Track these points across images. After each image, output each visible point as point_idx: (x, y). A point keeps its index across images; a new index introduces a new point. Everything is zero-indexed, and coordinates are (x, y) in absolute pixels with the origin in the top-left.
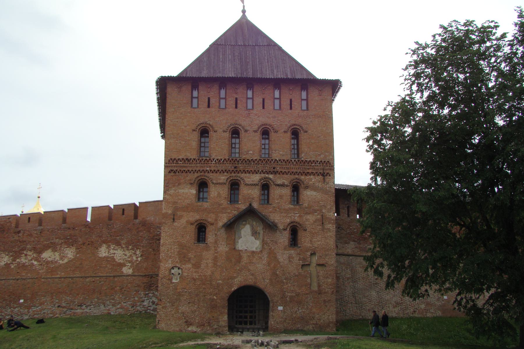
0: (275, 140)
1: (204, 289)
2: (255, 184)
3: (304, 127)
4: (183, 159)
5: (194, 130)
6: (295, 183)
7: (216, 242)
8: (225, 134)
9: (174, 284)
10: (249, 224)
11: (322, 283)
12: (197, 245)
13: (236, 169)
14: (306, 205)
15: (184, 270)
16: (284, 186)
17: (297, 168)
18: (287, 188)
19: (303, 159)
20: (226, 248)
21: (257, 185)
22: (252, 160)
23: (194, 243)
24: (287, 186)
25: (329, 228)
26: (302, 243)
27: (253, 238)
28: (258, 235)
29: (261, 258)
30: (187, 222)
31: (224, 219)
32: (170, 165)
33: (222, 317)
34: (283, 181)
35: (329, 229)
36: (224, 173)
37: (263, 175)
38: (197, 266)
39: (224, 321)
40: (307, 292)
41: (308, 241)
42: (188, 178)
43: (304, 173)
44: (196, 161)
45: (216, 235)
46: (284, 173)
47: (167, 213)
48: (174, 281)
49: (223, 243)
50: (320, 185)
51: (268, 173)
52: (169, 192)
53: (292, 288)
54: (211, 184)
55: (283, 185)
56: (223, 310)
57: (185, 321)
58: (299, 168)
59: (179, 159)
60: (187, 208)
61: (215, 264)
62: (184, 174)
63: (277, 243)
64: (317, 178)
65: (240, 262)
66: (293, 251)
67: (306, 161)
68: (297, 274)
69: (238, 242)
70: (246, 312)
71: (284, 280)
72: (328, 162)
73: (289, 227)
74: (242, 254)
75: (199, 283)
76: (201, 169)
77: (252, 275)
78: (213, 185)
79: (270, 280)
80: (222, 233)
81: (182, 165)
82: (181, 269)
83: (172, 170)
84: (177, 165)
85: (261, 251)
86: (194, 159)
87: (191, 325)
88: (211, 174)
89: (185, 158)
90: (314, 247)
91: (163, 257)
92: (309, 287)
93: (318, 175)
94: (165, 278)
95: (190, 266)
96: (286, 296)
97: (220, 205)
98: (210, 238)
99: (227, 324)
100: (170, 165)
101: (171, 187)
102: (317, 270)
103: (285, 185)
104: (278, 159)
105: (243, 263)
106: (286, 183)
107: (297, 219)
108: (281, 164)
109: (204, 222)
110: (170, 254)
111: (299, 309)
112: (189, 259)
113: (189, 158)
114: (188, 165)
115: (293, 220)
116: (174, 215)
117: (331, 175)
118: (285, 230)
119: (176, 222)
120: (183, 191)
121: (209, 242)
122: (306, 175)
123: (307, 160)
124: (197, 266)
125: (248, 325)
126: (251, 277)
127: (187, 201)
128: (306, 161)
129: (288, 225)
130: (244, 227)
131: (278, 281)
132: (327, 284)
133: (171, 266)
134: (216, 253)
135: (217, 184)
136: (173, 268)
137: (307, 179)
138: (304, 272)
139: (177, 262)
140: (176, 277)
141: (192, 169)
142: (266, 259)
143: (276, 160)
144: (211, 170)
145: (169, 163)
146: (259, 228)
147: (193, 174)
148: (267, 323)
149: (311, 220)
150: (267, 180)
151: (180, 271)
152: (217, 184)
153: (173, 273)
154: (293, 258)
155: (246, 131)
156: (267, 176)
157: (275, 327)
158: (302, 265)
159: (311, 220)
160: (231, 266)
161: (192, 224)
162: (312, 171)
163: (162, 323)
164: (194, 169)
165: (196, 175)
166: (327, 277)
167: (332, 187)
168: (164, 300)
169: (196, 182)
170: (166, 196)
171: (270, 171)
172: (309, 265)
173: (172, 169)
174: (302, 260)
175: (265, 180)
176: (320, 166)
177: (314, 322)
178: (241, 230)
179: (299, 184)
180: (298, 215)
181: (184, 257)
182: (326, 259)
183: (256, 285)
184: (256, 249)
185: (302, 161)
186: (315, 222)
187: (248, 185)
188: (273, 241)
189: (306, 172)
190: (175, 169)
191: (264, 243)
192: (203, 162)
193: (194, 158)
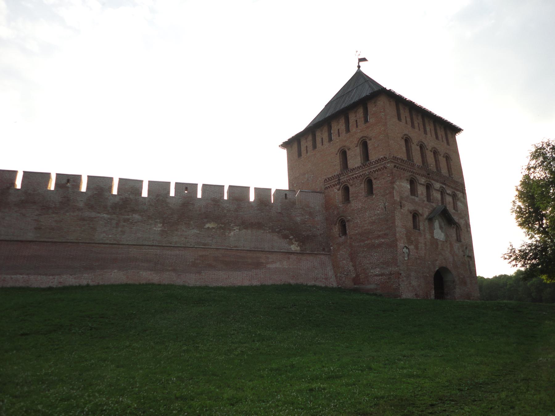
31: (425, 212)
38: (417, 248)
48: (406, 259)
49: (428, 232)
77: (445, 259)
80: (426, 223)
81: (401, 163)
86: (406, 161)
114: (403, 164)
124: (417, 248)
133: (402, 245)
134: (425, 239)
161: (411, 213)
165: (410, 174)
184: (443, 239)
191: (447, 236)
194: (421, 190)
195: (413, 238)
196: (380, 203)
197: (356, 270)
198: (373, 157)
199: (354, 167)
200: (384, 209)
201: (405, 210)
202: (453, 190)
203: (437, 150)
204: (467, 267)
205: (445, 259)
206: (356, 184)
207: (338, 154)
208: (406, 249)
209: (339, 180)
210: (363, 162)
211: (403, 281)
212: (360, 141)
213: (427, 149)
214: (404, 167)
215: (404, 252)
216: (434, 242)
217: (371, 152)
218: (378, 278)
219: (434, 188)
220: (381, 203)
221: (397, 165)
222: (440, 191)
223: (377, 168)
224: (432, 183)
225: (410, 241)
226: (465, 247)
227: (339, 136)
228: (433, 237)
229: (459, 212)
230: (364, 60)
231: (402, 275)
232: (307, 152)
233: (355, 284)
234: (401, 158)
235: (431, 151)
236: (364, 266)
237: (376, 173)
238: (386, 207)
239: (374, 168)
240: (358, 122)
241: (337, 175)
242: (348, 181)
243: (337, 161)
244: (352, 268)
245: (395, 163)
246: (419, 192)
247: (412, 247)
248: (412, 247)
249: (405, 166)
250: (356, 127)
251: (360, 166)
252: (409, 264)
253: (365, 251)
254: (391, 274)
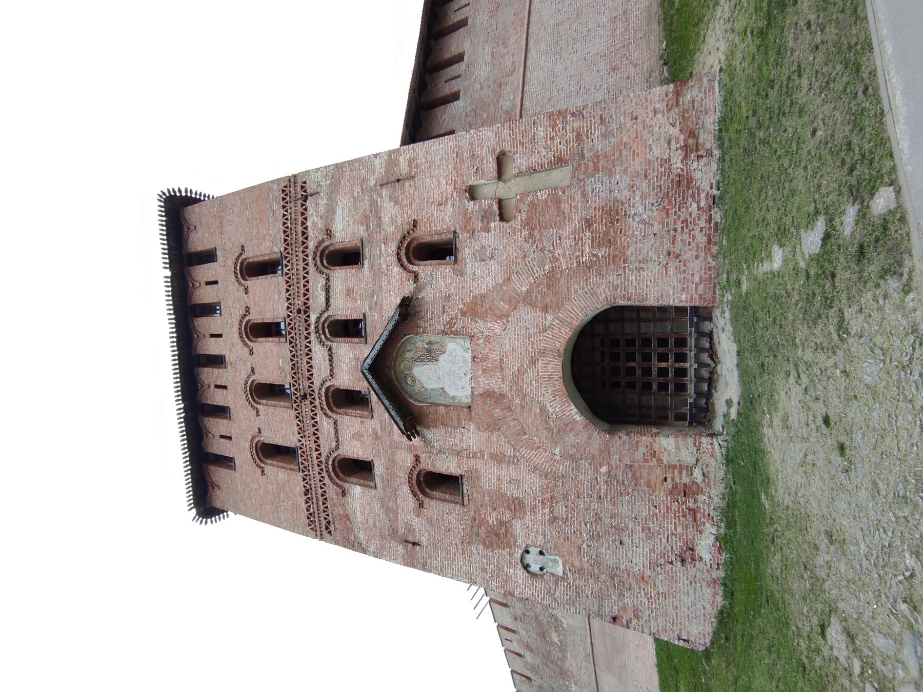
0: (260, 312)
1: (579, 497)
2: (330, 355)
3: (237, 252)
4: (307, 502)
5: (263, 472)
6: (325, 262)
7: (458, 454)
8: (261, 412)
9: (570, 575)
10: (410, 369)
11: (550, 155)
12: (466, 499)
13: (308, 396)
14: (362, 228)
15: (529, 542)
16: (329, 286)
17: (297, 260)
18: (331, 278)
19: (282, 249)
20: (469, 431)
21: (330, 349)
22: (292, 360)
23: (464, 505)
24: (328, 279)
25: (407, 163)
26: (445, 227)
27: (441, 358)
28: (435, 347)
29: (488, 339)
30: (418, 516)
32: (318, 528)
33: (666, 454)
34: (319, 289)
35: (410, 162)
36: (316, 422)
37: (313, 337)
39: (678, 448)
40: (578, 196)
41: (440, 211)
42: (335, 497)
43: (303, 243)
44: (306, 475)
45: (440, 452)
46: (306, 288)
47: (403, 556)
48: (559, 571)
49: (458, 436)
50: (323, 201)
51: (309, 325)
52: (364, 542)
53: (568, 243)
54: (340, 452)
55: (327, 290)
56: (642, 449)
57: (679, 564)
58: (297, 256)
59: (308, 510)
60: (391, 512)
61: (514, 461)
62: (328, 504)
63: (449, 296)
64: (311, 212)
65: (502, 396)
66: (467, 251)
67: (284, 242)
68: (525, 233)
69: (453, 397)
70: (647, 372)
71: (547, 268)
72: (283, 191)
73: (410, 267)
74: (481, 391)
75: (564, 509)
76: (317, 469)
77: (533, 362)
78: (341, 447)
79: (545, 309)
80: (434, 435)
81: (315, 503)
82: (526, 547)
83: (327, 528)
84: (316, 516)
85: (471, 337)
86: (304, 479)
87: (692, 550)
88: (322, 449)
89: (305, 498)
90: (455, 194)
91: (499, 585)
92: (564, 192)
93: (306, 209)
94: (552, 592)
95: (518, 527)
96: (594, 259)
97: (376, 436)
98: (448, 466)
99: (690, 440)
100: (318, 528)
101: (354, 535)
102: (517, 176)
103: (326, 284)
104: (286, 304)
105: (505, 388)
106: (322, 282)
107: (393, 247)
108: (292, 296)
109: (415, 476)
110: (492, 566)
111: (635, 214)
112: (501, 523)
113: (304, 490)
115: (395, 259)
116: (406, 541)
117: (304, 180)
118: (416, 277)
119: (419, 540)
120: (358, 514)
121: (458, 470)
122: (306, 238)
123: (283, 240)
124: (517, 506)
125: (687, 365)
126: (540, 366)
127: (377, 506)
128: (285, 240)
129: (405, 268)
130: (419, 381)
131: (548, 286)
132: (552, 138)
133: (521, 572)
134: (483, 456)
135: (337, 437)
136: (526, 567)
137: (314, 234)
138: (520, 212)
139: (511, 555)
140: (550, 564)
141: (319, 488)
142: (489, 325)
143: (288, 308)
144: (317, 450)
145: (316, 531)
146: (419, 345)
147: (327, 486)
148: (680, 310)
149: (394, 212)
150: (320, 327)
151: (534, 551)
152: (338, 440)
153: (538, 569)
154: (483, 247)
155: (253, 371)
156: (312, 327)
157: (701, 287)
158: (502, 218)
159: (394, 212)
160: (515, 419)
161: (421, 505)
162: (300, 223)
163: (688, 633)
164: (319, 484)
166: (533, 141)
167: (325, 173)
168: (616, 608)
169: (340, 483)
170: (372, 548)
171: (305, 319)
172: (500, 202)
173: (324, 527)
174: (488, 223)
175: (321, 332)
176: (291, 208)
177: (680, 157)
178: (426, 389)
179: (327, 251)
180: (383, 248)
181: (497, 535)
182: (484, 154)
183: (562, 350)
185: (286, 249)
186: (396, 202)
187: (331, 370)
188: (444, 307)
189: (301, 239)
190: (324, 522)
191: (450, 331)
192: (306, 464)
193: (302, 479)
229: (361, 231)
252: (577, 563)
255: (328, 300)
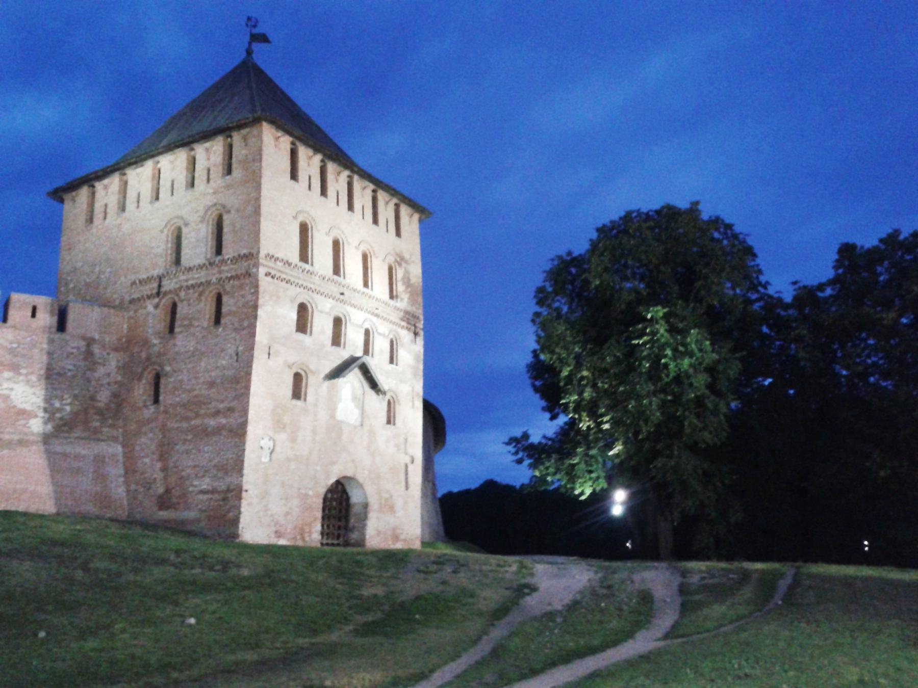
38: (293, 440)
81: (282, 269)
124: (293, 440)
161: (290, 367)
165: (298, 290)
194: (322, 325)
195: (286, 419)
196: (229, 345)
197: (165, 478)
198: (229, 251)
199: (192, 265)
200: (235, 358)
201: (277, 362)
202: (395, 327)
203: (372, 247)
204: (402, 476)
205: (353, 461)
206: (192, 301)
207: (166, 231)
208: (270, 440)
209: (160, 286)
210: (209, 256)
211: (250, 504)
212: (209, 213)
213: (349, 243)
214: (288, 278)
215: (262, 448)
216: (336, 427)
217: (227, 238)
218: (206, 497)
219: (350, 320)
220: (232, 344)
221: (273, 272)
222: (362, 328)
223: (234, 273)
224: (347, 312)
225: (278, 424)
226: (402, 439)
227: (172, 194)
228: (333, 416)
230: (263, 38)
231: (250, 492)
232: (105, 218)
233: (160, 508)
234: (285, 259)
235: (357, 248)
236: (183, 471)
237: (231, 282)
238: (240, 354)
239: (228, 272)
240: (211, 172)
241: (158, 276)
242: (178, 291)
243: (161, 246)
244: (159, 475)
245: (266, 266)
246: (316, 328)
247: (282, 437)
248: (282, 437)
249: (292, 275)
250: (205, 182)
251: (204, 265)
253: (189, 441)
254: (229, 490)
255: (380, 334)
